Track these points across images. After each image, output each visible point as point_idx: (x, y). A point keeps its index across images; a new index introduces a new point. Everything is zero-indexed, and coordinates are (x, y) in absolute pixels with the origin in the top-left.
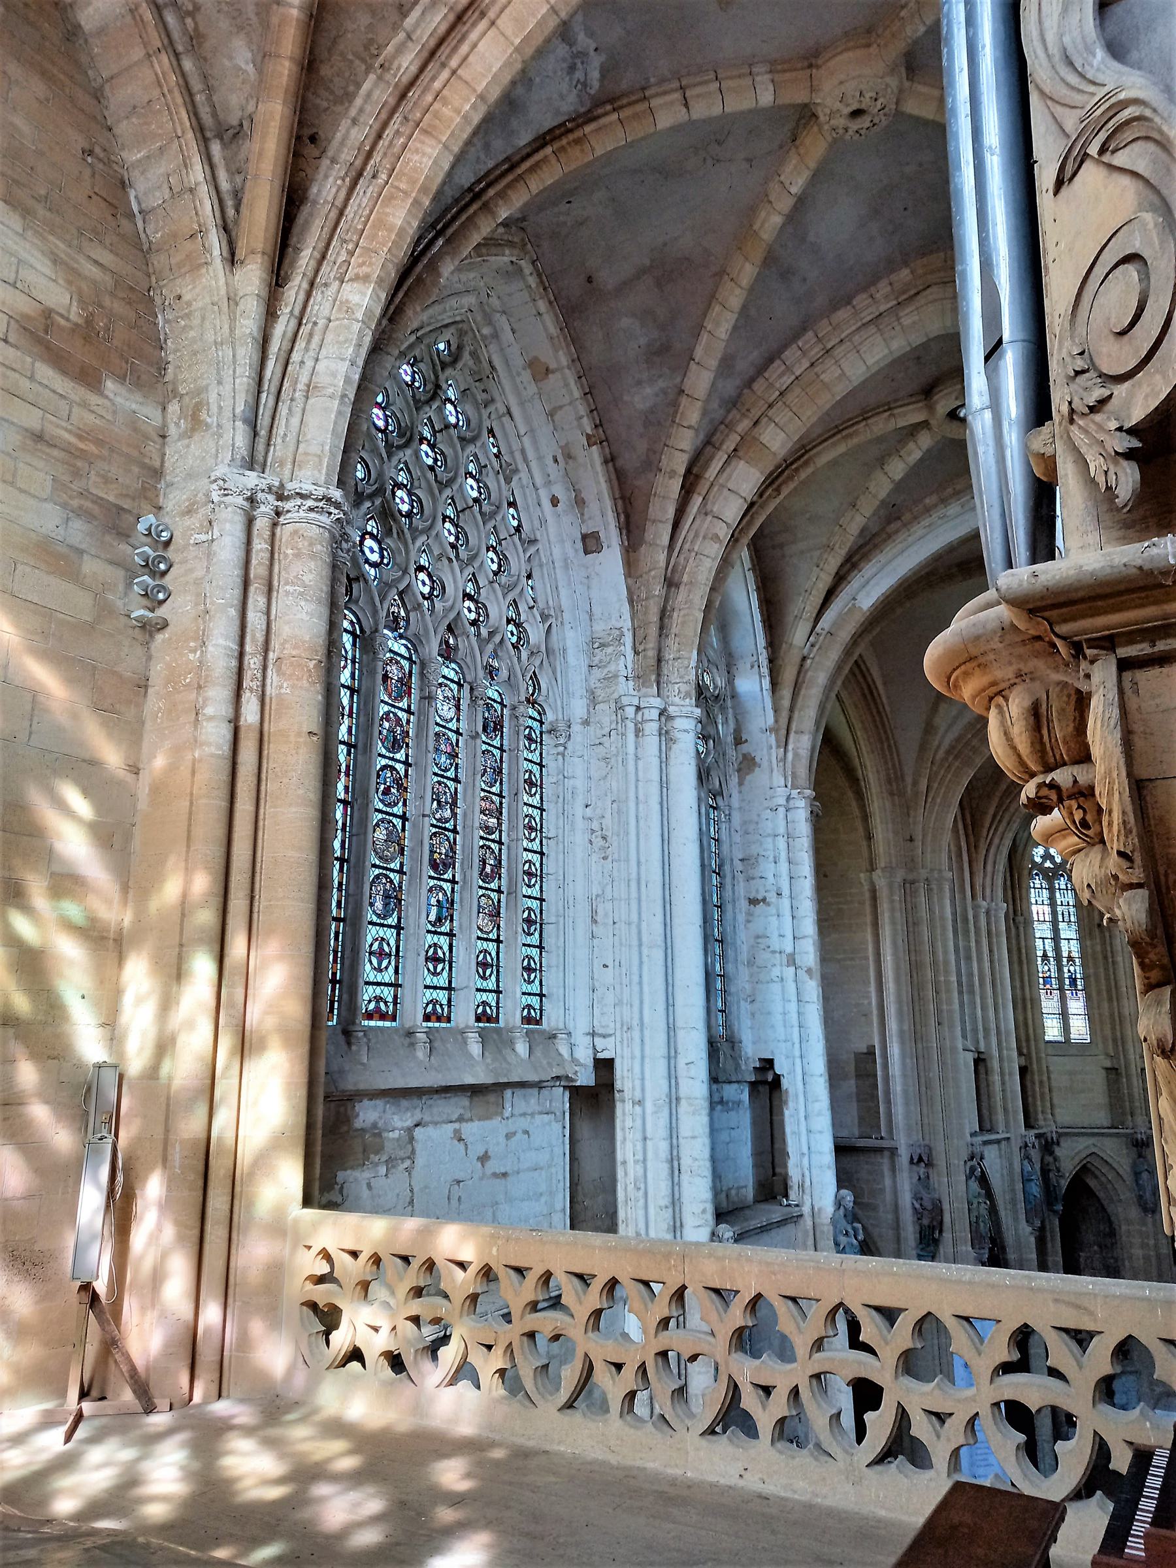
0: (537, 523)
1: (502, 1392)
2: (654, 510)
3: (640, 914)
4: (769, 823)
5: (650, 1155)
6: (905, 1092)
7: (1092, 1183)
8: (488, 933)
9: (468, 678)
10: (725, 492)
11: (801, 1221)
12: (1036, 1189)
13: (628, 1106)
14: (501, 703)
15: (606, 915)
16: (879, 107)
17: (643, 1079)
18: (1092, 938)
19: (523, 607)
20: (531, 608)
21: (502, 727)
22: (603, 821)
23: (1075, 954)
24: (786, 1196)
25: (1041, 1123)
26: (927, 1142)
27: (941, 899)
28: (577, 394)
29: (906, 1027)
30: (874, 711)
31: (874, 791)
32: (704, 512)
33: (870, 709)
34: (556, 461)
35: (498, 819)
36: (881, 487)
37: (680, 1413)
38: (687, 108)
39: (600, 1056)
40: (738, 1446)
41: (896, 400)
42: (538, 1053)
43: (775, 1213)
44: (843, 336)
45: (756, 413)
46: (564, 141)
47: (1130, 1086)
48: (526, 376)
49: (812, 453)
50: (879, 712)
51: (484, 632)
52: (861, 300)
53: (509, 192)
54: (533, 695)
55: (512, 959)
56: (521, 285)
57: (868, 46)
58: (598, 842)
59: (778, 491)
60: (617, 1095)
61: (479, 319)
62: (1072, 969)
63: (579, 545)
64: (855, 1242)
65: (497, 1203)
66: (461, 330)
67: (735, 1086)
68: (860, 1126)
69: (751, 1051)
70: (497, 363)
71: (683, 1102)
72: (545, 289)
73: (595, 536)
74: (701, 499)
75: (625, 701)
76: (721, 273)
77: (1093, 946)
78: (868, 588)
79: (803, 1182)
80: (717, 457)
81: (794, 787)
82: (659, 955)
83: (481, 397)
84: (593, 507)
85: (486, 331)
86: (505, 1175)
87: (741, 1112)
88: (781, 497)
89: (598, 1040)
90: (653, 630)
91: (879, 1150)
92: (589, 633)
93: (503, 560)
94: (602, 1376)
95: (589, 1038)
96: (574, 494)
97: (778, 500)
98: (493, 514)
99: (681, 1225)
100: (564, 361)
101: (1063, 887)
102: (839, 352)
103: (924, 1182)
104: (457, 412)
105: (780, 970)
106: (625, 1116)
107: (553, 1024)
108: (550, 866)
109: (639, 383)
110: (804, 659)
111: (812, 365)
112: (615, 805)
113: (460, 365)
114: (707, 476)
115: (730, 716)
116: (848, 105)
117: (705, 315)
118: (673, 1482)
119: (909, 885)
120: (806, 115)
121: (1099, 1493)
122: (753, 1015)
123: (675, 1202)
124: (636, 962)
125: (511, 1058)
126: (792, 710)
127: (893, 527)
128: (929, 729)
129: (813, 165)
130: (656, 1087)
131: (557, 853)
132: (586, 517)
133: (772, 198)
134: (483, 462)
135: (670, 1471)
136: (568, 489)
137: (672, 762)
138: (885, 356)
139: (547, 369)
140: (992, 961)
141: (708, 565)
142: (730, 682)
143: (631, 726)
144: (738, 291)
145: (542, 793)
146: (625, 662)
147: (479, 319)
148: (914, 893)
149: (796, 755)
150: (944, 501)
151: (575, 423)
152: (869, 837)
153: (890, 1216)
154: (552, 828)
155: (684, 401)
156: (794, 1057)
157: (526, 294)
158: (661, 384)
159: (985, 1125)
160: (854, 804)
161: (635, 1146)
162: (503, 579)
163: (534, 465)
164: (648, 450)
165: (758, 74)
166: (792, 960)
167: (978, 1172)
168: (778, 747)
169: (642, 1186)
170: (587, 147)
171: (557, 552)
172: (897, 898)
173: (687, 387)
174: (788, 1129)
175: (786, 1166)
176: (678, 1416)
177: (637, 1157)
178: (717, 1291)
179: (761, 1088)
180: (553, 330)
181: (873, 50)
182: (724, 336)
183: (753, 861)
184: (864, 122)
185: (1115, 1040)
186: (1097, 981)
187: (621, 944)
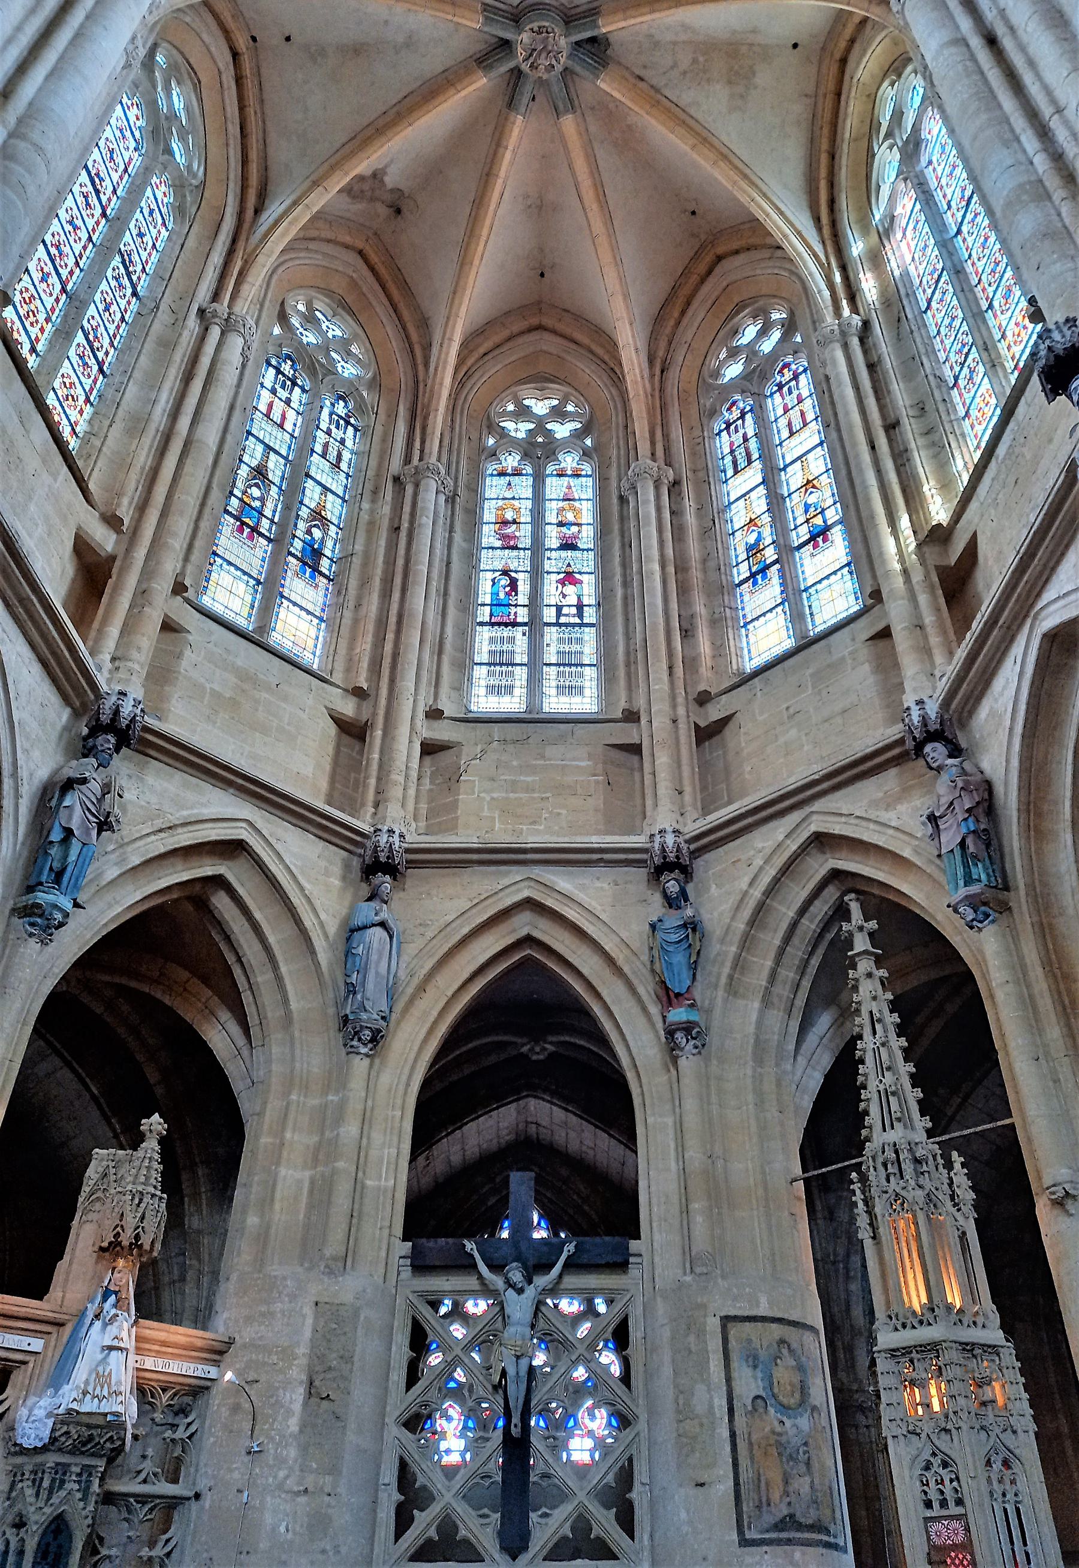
18: (373, 501)
62: (317, 533)
77: (372, 511)
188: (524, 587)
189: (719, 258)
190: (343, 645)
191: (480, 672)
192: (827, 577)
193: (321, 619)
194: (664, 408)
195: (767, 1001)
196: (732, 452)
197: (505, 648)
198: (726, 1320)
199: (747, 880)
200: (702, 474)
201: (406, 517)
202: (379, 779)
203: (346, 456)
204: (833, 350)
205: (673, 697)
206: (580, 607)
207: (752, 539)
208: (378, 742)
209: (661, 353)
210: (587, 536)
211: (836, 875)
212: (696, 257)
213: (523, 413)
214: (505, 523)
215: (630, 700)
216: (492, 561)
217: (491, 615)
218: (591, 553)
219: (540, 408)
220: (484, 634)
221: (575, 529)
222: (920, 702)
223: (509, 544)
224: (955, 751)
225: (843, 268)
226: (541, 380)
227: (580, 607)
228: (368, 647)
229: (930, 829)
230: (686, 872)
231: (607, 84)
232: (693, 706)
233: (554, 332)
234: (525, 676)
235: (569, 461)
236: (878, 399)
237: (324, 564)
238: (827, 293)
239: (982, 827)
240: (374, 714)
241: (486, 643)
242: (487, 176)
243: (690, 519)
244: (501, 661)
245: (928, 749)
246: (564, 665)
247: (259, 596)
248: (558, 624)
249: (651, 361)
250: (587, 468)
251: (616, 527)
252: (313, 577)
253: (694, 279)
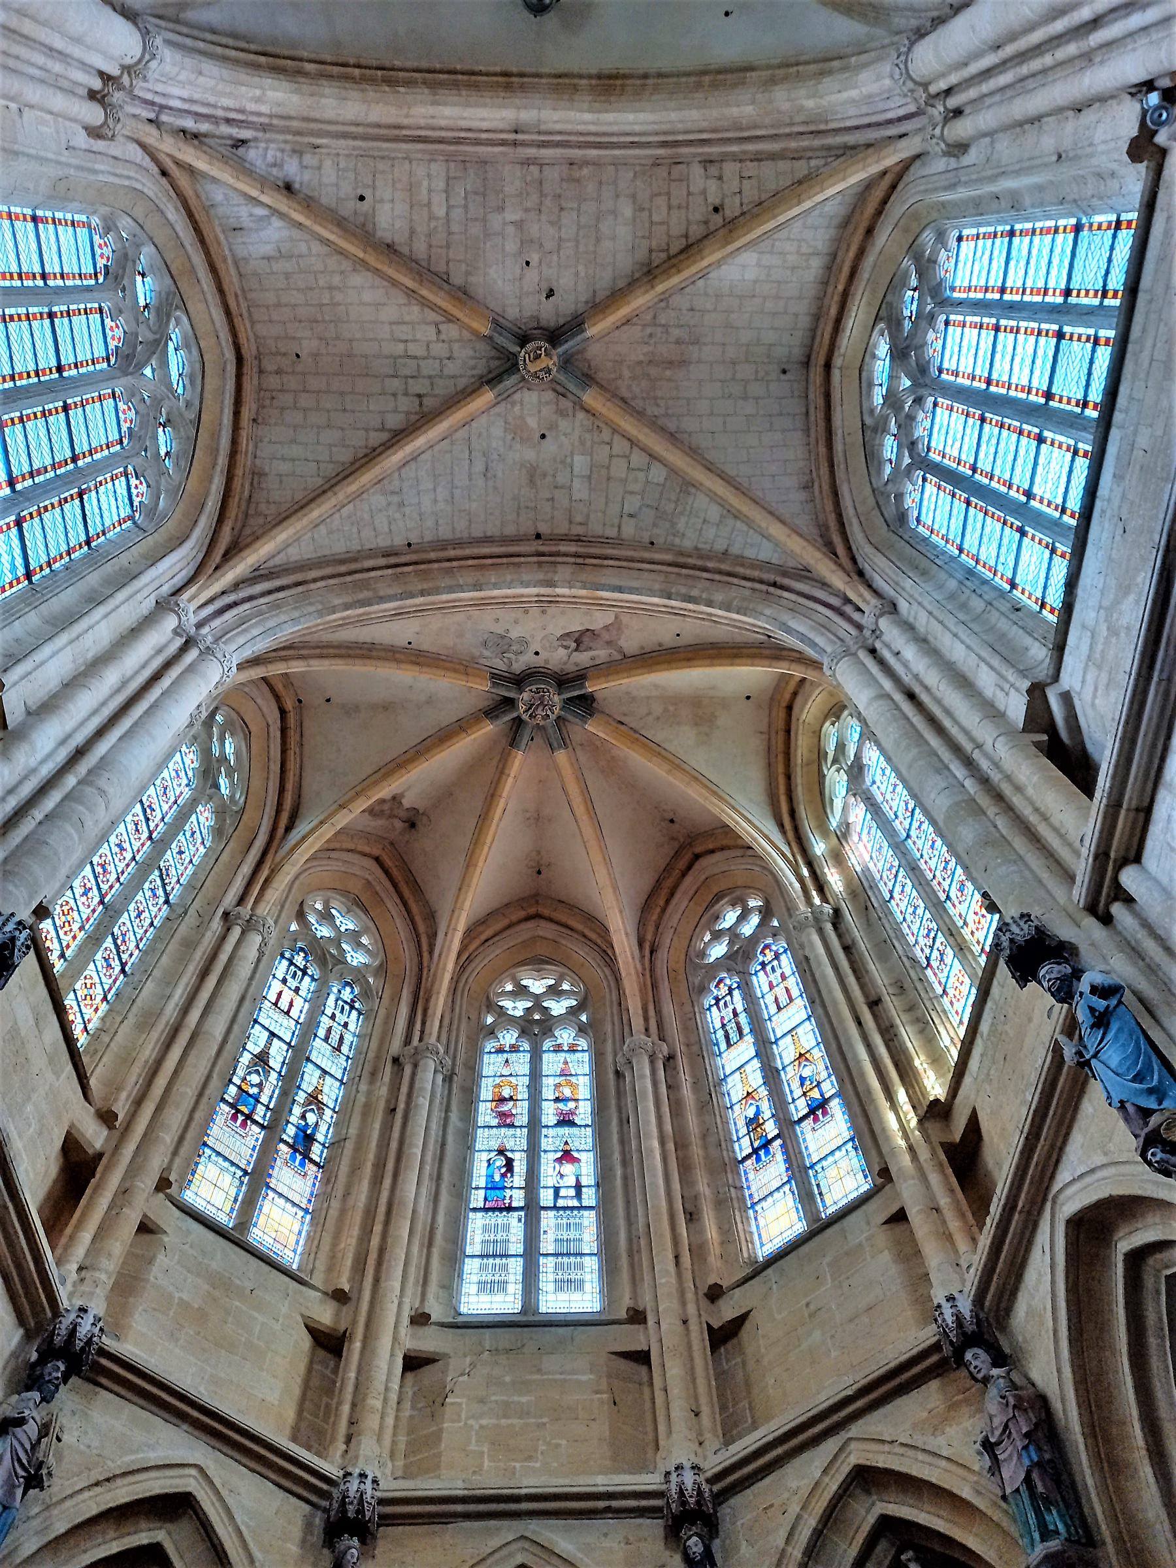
18: (372, 1082)
62: (311, 1118)
77: (369, 1093)
101: (347, 994)
186: (359, 1147)
188: (520, 1167)
189: (697, 857)
190: (327, 1239)
191: (471, 1267)
192: (832, 1153)
193: (306, 1211)
194: (654, 986)
196: (723, 1026)
197: (499, 1237)
199: (783, 1534)
200: (695, 1048)
201: (403, 1098)
202: (354, 1405)
203: (348, 1038)
204: (809, 935)
205: (682, 1293)
206: (578, 1187)
207: (751, 1113)
208: (355, 1357)
209: (649, 937)
210: (584, 1113)
211: (887, 1526)
212: (677, 855)
213: (521, 991)
214: (502, 1100)
215: (635, 1295)
216: (486, 1140)
217: (486, 1199)
218: (589, 1130)
219: (537, 986)
220: (477, 1224)
221: (572, 1105)
222: (950, 1298)
223: (506, 1122)
224: (1000, 1359)
225: (810, 865)
226: (538, 963)
227: (578, 1187)
228: (353, 1242)
229: (987, 1461)
230: (710, 1526)
231: (591, 727)
232: (704, 1302)
233: (551, 920)
234: (520, 1270)
235: (565, 1036)
236: (858, 978)
237: (316, 1151)
238: (797, 885)
239: (1047, 1456)
240: (354, 1322)
241: (479, 1232)
242: (492, 796)
243: (687, 1092)
244: (495, 1253)
245: (968, 1356)
246: (562, 1255)
247: (244, 1188)
248: (555, 1208)
249: (641, 944)
250: (583, 1043)
251: (613, 1102)
252: (302, 1164)
253: (676, 873)
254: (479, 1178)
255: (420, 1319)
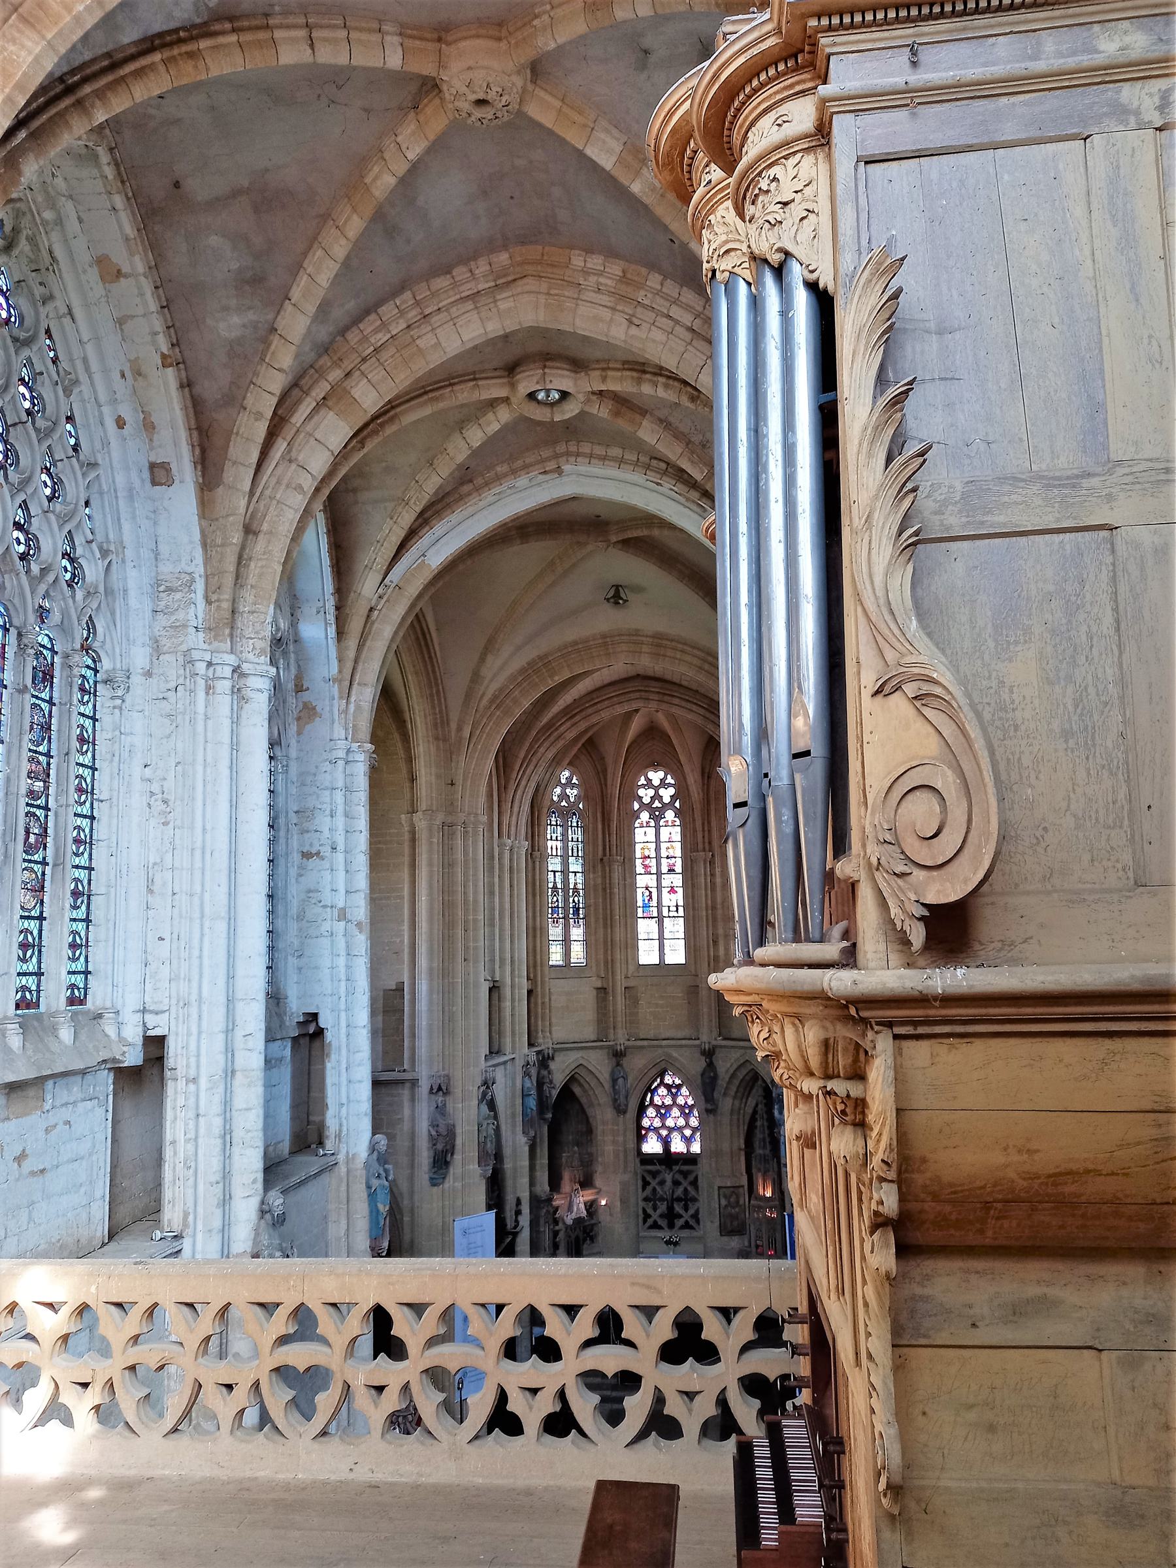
0: (98, 445)
1: (97, 1426)
2: (235, 451)
3: (203, 886)
4: (328, 776)
5: (202, 1131)
6: (430, 1026)
7: (577, 1090)
8: (30, 910)
9: (16, 622)
10: (312, 441)
11: (336, 1168)
12: (532, 1103)
13: (181, 1084)
14: (52, 650)
15: (164, 884)
16: (503, 103)
17: (198, 1056)
19: (79, 540)
20: (89, 542)
21: (52, 677)
22: (165, 784)
23: (580, 886)
24: (321, 1143)
25: (540, 1041)
26: (446, 1072)
27: (475, 842)
28: (153, 306)
29: (435, 965)
30: (426, 656)
31: (420, 734)
32: (288, 458)
33: (422, 653)
34: (123, 376)
35: (45, 782)
36: (459, 450)
37: (294, 1422)
38: (313, 49)
39: (150, 1033)
40: (350, 1444)
41: (483, 371)
42: (83, 1036)
43: (309, 1163)
44: (441, 305)
45: (348, 365)
46: (176, 51)
47: (615, 1004)
48: (93, 274)
49: (398, 410)
50: (430, 657)
51: (35, 568)
52: (460, 272)
53: (109, 94)
54: (87, 639)
55: (56, 939)
56: (95, 172)
57: (499, 39)
58: (158, 806)
59: (362, 443)
60: (168, 1074)
61: (40, 199)
63: (146, 475)
64: (386, 1183)
65: (33, 1203)
66: (18, 210)
67: (279, 1042)
68: (383, 1060)
69: (296, 1007)
70: (59, 253)
71: (238, 1075)
72: (123, 182)
73: (165, 467)
74: (285, 444)
75: (196, 655)
76: (325, 217)
77: (594, 879)
78: (439, 545)
79: (340, 1131)
80: (305, 403)
81: (354, 741)
82: (222, 926)
83: (38, 291)
84: (164, 434)
85: (48, 215)
86: (42, 1171)
87: (283, 1068)
88: (365, 450)
89: (148, 1017)
90: (229, 580)
91: (401, 1082)
92: (153, 574)
93: (57, 484)
94: (212, 1397)
95: (140, 1015)
96: (142, 416)
97: (362, 454)
98: (49, 432)
99: (230, 1197)
100: (140, 267)
102: (435, 320)
103: (441, 1110)
104: (9, 305)
105: (329, 923)
106: (176, 1094)
107: (99, 1003)
108: (101, 831)
109: (226, 309)
110: (371, 609)
111: (409, 327)
112: (179, 768)
113: (15, 252)
114: (293, 420)
115: (292, 661)
116: (474, 92)
117: (305, 254)
118: (287, 1487)
119: (447, 829)
120: (430, 87)
121: (654, 1433)
122: (300, 969)
123: (226, 1176)
124: (197, 935)
125: (54, 1046)
126: (356, 661)
127: (466, 488)
128: (476, 677)
129: (432, 137)
130: (211, 1061)
131: (110, 817)
132: (156, 443)
133: (387, 155)
134: (38, 367)
135: (281, 1476)
136: (135, 410)
137: (243, 721)
138: (480, 335)
139: (119, 271)
140: (511, 896)
141: (291, 517)
142: (294, 624)
143: (201, 683)
144: (343, 242)
145: (94, 750)
146: (198, 611)
147: (40, 199)
148: (452, 835)
149: (358, 708)
150: (514, 472)
151: (148, 338)
152: (413, 779)
153: (407, 1144)
154: (105, 788)
155: (276, 341)
156: (339, 1011)
157: (99, 182)
158: (251, 316)
159: (494, 1050)
160: (399, 745)
161: (186, 1124)
162: (58, 506)
163: (97, 377)
164: (232, 383)
165: (388, 33)
166: (343, 915)
167: (489, 1097)
168: (341, 698)
169: (193, 1164)
170: (201, 64)
171: (120, 479)
172: (435, 840)
173: (281, 324)
174: (330, 1079)
175: (323, 1114)
176: (291, 1425)
177: (188, 1136)
178: (334, 1305)
179: (302, 1041)
180: (130, 231)
181: (503, 45)
182: (325, 284)
183: (309, 813)
184: (486, 113)
185: (606, 962)
187: (181, 917)
195: (735, 1098)
198: (719, 1188)
210: (678, 868)
216: (642, 881)
219: (656, 776)
226: (655, 766)
227: (677, 906)
235: (670, 815)
243: (718, 880)
254: (640, 903)
255: (626, 977)
